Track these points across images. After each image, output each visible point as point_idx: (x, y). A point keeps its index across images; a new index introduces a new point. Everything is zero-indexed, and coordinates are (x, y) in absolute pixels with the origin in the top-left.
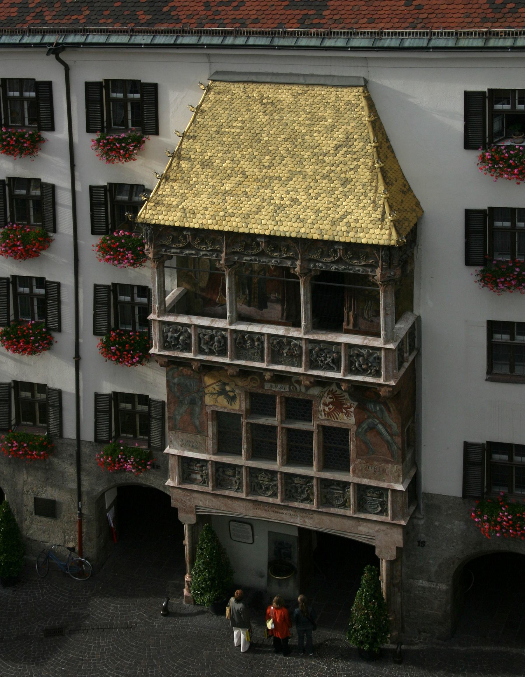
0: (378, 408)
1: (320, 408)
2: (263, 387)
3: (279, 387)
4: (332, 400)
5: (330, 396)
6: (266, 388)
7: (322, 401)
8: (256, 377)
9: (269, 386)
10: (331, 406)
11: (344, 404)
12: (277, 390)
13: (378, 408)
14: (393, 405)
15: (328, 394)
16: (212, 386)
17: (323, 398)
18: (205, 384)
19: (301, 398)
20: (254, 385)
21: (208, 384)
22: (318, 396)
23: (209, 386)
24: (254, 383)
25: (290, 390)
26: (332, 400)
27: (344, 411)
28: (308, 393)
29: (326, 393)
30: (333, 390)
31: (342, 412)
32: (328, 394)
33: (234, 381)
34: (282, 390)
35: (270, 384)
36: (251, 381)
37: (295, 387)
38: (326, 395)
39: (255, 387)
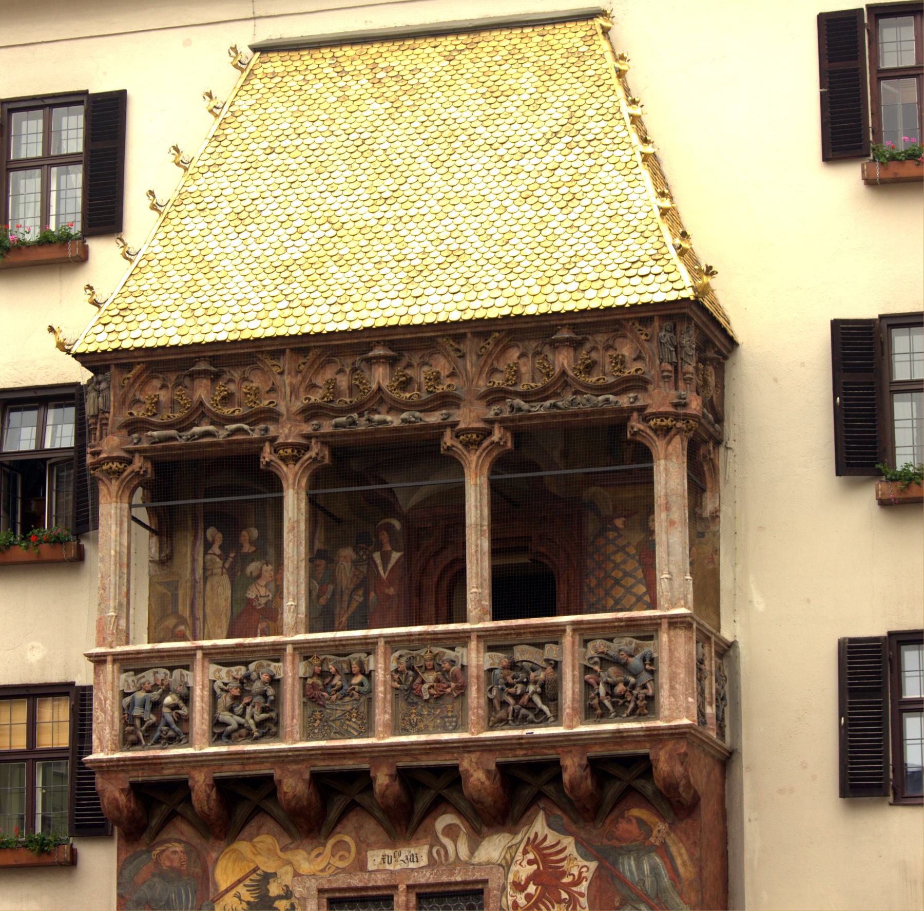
0: (646, 867)
1: (504, 899)
2: (361, 865)
3: (403, 857)
4: (535, 867)
5: (531, 856)
6: (371, 866)
7: (511, 877)
8: (347, 839)
9: (379, 860)
10: (532, 889)
11: (564, 874)
12: (398, 867)
13: (646, 867)
14: (683, 851)
15: (525, 852)
16: (234, 892)
17: (514, 868)
18: (216, 889)
19: (459, 879)
20: (341, 864)
21: (223, 887)
22: (500, 865)
23: (227, 891)
24: (342, 858)
25: (432, 863)
26: (535, 867)
27: (564, 895)
28: (476, 860)
29: (521, 849)
30: (536, 834)
31: (560, 901)
32: (525, 852)
33: (290, 863)
34: (412, 865)
35: (381, 852)
36: (333, 855)
37: (445, 848)
38: (519, 856)
39: (344, 870)
